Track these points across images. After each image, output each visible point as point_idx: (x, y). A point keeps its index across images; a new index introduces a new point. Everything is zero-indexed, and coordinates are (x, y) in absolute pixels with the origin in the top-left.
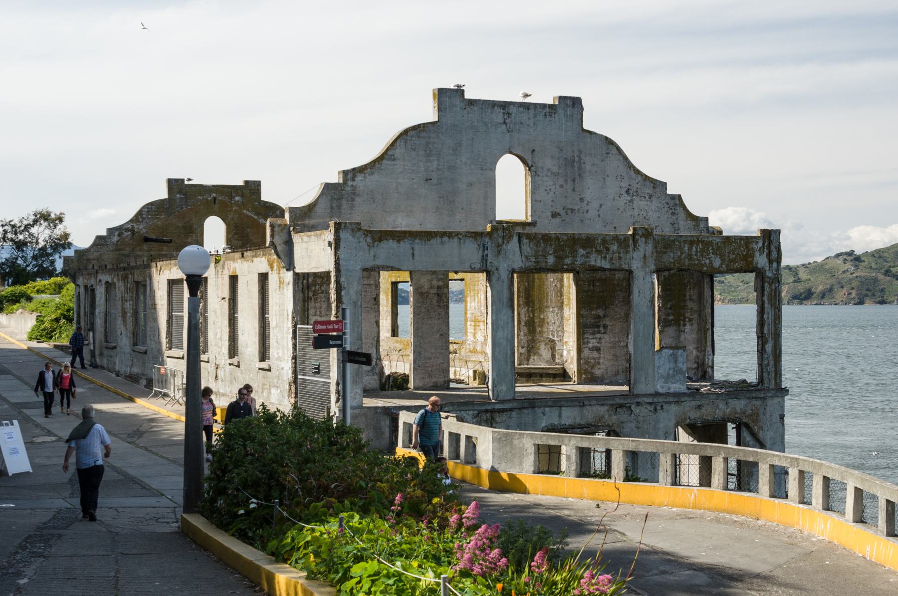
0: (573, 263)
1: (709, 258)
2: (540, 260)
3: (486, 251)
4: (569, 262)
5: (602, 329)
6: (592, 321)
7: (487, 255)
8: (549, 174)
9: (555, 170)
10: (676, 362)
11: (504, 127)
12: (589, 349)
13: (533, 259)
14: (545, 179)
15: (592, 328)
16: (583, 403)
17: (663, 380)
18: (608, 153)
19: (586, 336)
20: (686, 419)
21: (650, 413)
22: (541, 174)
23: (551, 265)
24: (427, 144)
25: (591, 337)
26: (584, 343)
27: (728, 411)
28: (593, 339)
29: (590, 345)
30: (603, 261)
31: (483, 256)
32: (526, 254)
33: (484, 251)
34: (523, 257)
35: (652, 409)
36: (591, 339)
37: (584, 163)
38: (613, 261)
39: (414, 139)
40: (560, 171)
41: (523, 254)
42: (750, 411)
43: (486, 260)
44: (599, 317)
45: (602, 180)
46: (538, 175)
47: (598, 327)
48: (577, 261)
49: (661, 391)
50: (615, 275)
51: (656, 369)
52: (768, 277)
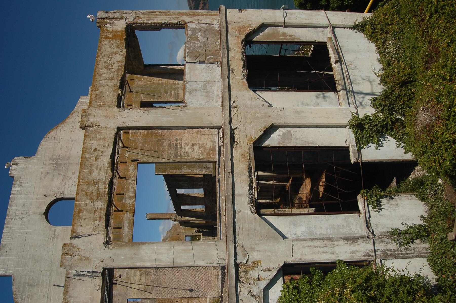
0: (104, 183)
1: (114, 63)
2: (98, 216)
3: (85, 273)
4: (103, 186)
5: (178, 142)
6: (172, 149)
7: (88, 272)
8: (64, 183)
9: (61, 178)
10: (196, 90)
11: (25, 219)
12: (192, 151)
13: (97, 222)
14: (67, 186)
15: (177, 150)
16: (229, 173)
17: (211, 100)
18: (55, 138)
19: (183, 154)
20: (243, 83)
21: (239, 112)
22: (63, 190)
23: (104, 205)
24: (29, 285)
25: (183, 151)
26: (188, 156)
27: (237, 49)
28: (185, 149)
29: (190, 151)
30: (105, 154)
31: (89, 276)
32: (91, 230)
33: (84, 275)
34: (94, 233)
35: (235, 110)
36: (185, 150)
37: (59, 156)
38: (107, 145)
39: (24, 297)
40: (63, 174)
41: (91, 233)
42: (237, 33)
43: (94, 272)
44: (170, 144)
45: (73, 143)
46: (63, 191)
47: (176, 145)
48: (103, 179)
49: (220, 102)
50: (141, 133)
51: (202, 107)
52: (134, 20)
